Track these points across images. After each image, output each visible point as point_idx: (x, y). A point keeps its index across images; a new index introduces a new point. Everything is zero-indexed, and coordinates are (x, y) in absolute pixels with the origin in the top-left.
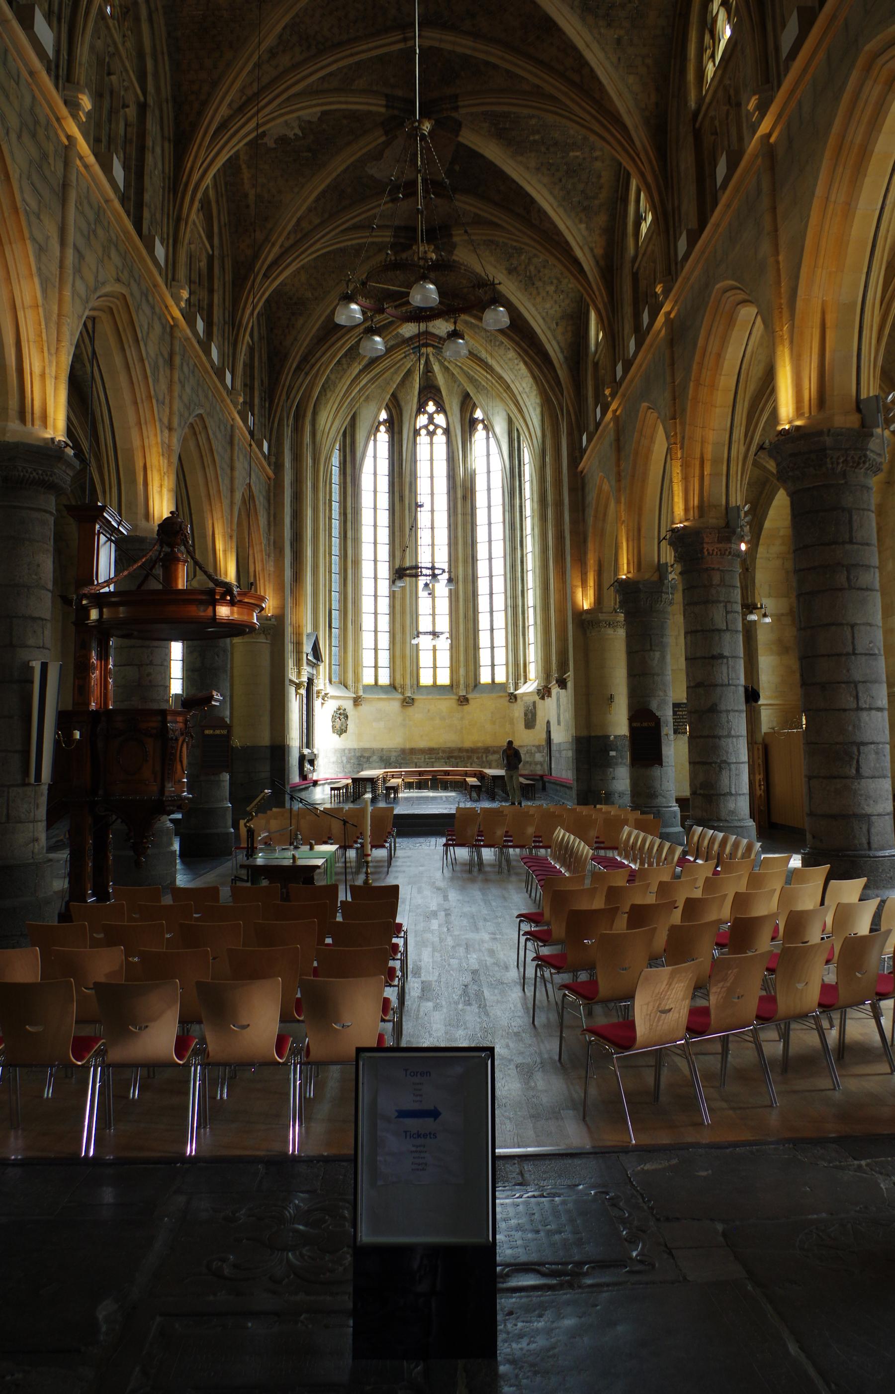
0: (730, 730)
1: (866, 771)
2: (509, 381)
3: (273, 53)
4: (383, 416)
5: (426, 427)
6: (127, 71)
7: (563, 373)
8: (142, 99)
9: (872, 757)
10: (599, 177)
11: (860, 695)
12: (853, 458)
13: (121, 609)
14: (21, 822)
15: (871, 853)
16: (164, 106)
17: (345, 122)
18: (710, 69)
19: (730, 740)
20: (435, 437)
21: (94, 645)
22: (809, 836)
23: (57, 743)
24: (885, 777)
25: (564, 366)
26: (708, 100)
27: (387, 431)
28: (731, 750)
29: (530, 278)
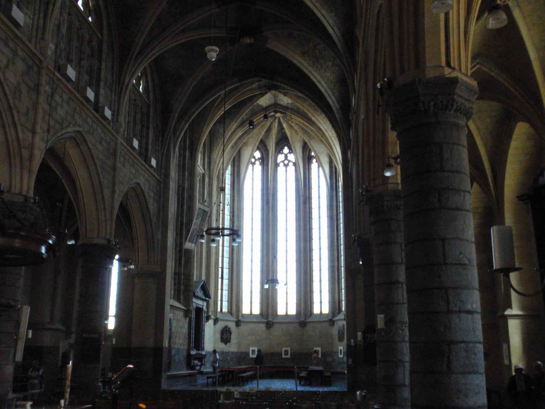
2: (323, 129)
5: (283, 162)
12: (442, 101)
20: (288, 167)
25: (340, 112)
27: (260, 164)
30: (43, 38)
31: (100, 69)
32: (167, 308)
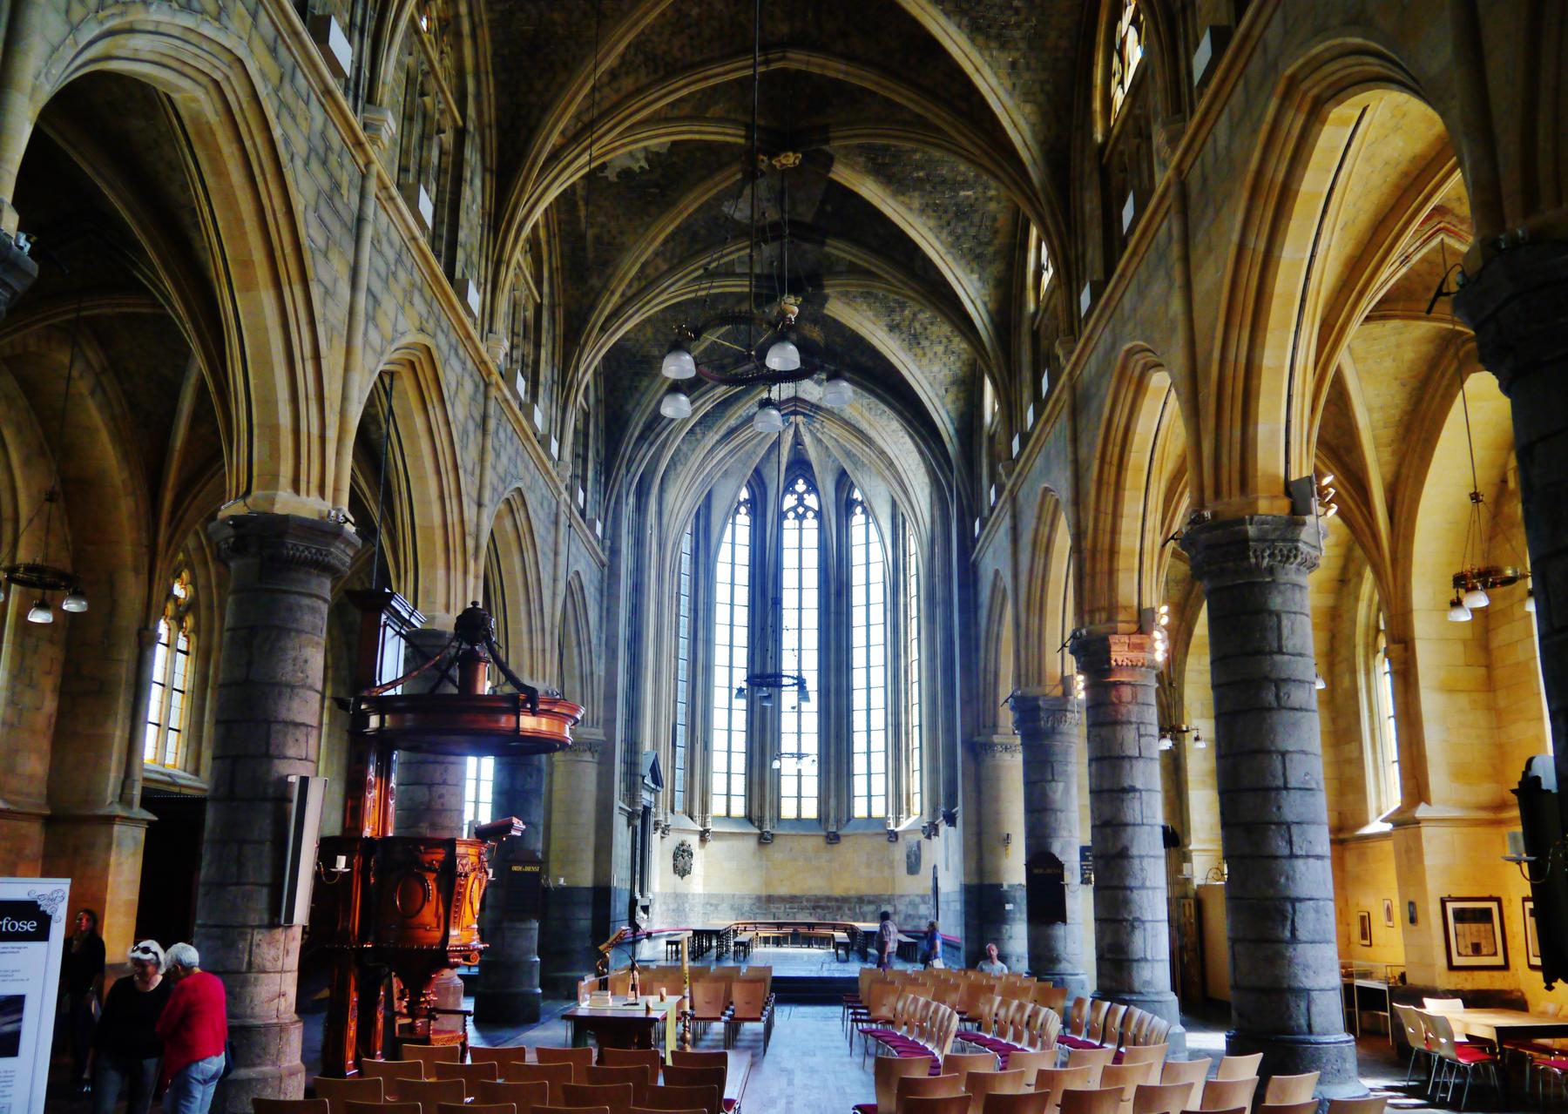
0: (1144, 880)
1: (1302, 934)
3: (613, 75)
4: (744, 494)
5: (794, 509)
6: (443, 92)
7: (952, 448)
8: (460, 123)
9: (1311, 915)
10: (994, 219)
11: (1294, 838)
13: (409, 716)
14: (265, 972)
15: (1312, 1038)
16: (487, 132)
17: (698, 154)
18: (1119, 96)
19: (1144, 892)
21: (373, 758)
22: (1234, 1014)
23: (317, 876)
24: (1328, 942)
25: (955, 440)
26: (1115, 131)
28: (1146, 905)
29: (915, 336)
30: (490, 331)
32: (616, 810)
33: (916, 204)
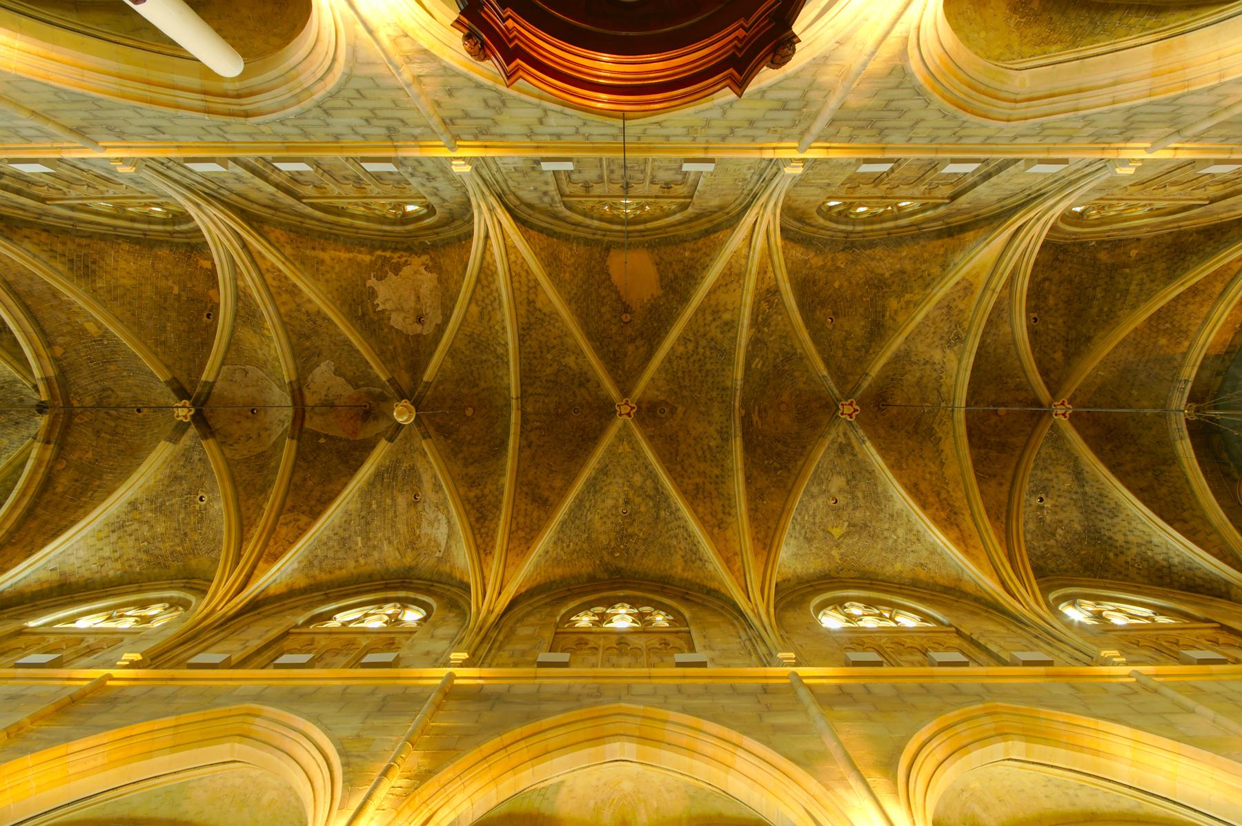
10: (341, 568)
17: (391, 347)
31: (266, 179)
33: (351, 507)
